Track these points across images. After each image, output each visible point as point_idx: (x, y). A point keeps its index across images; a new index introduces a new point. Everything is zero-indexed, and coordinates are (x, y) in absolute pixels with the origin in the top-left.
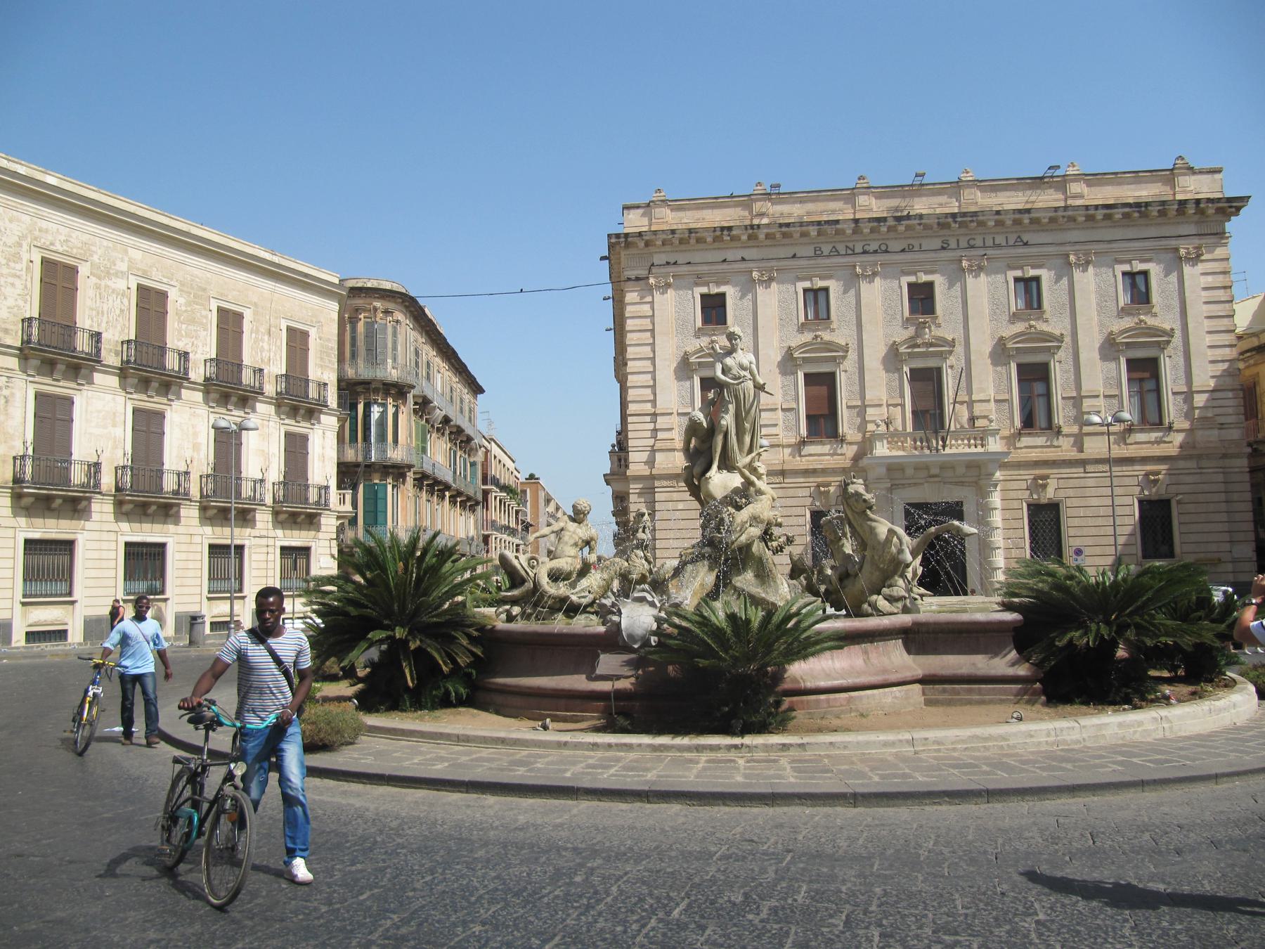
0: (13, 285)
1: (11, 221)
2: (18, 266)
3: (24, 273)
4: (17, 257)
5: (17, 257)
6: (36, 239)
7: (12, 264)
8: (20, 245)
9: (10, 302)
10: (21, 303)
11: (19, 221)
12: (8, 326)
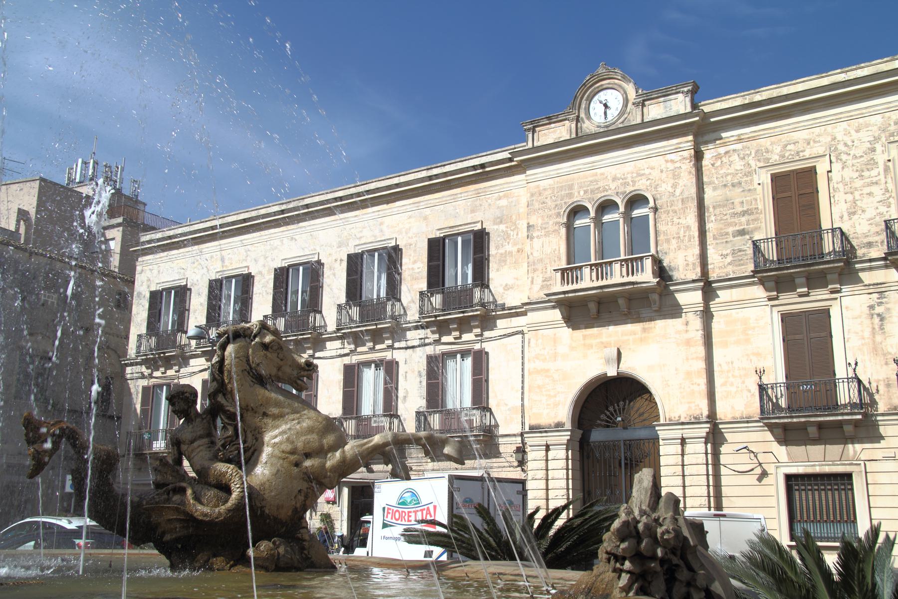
0: (870, 194)
1: (857, 131)
2: (874, 173)
3: (882, 177)
4: (873, 163)
5: (873, 163)
6: (892, 135)
7: (866, 174)
8: (873, 150)
9: (871, 213)
10: (882, 209)
11: (867, 125)
12: (871, 239)
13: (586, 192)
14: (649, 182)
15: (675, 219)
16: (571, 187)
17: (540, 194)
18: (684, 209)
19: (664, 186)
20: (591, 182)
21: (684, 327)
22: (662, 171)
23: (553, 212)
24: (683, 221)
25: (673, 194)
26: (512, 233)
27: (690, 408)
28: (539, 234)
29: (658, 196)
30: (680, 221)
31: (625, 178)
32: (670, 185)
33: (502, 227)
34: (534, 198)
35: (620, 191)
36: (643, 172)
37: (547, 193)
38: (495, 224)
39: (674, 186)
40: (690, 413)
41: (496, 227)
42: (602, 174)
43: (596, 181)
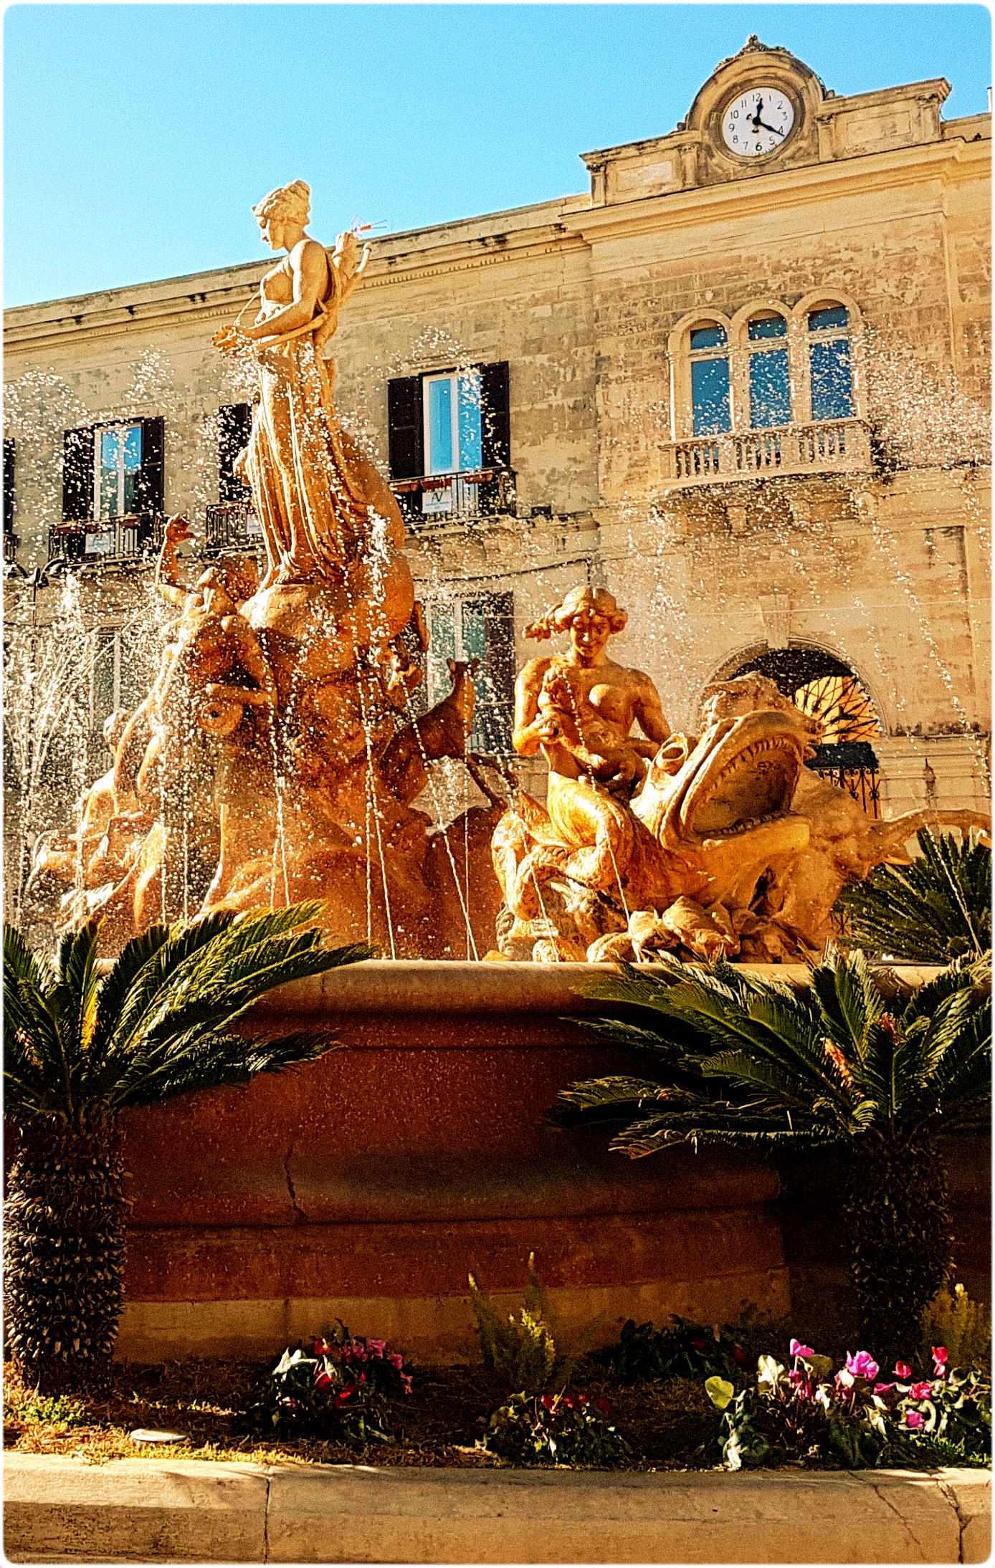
13: (716, 294)
14: (849, 276)
15: (907, 354)
16: (686, 284)
17: (621, 297)
18: (922, 332)
19: (881, 284)
20: (729, 274)
21: (926, 558)
22: (876, 255)
23: (650, 331)
24: (921, 354)
25: (900, 300)
26: (562, 370)
27: (939, 711)
28: (622, 374)
29: (869, 304)
30: (916, 353)
31: (800, 269)
32: (893, 283)
33: (542, 359)
34: (610, 304)
35: (788, 292)
36: (837, 256)
37: (635, 295)
38: (525, 353)
39: (902, 284)
40: (938, 719)
41: (528, 359)
42: (749, 259)
43: (738, 273)
